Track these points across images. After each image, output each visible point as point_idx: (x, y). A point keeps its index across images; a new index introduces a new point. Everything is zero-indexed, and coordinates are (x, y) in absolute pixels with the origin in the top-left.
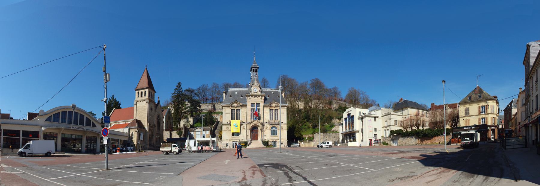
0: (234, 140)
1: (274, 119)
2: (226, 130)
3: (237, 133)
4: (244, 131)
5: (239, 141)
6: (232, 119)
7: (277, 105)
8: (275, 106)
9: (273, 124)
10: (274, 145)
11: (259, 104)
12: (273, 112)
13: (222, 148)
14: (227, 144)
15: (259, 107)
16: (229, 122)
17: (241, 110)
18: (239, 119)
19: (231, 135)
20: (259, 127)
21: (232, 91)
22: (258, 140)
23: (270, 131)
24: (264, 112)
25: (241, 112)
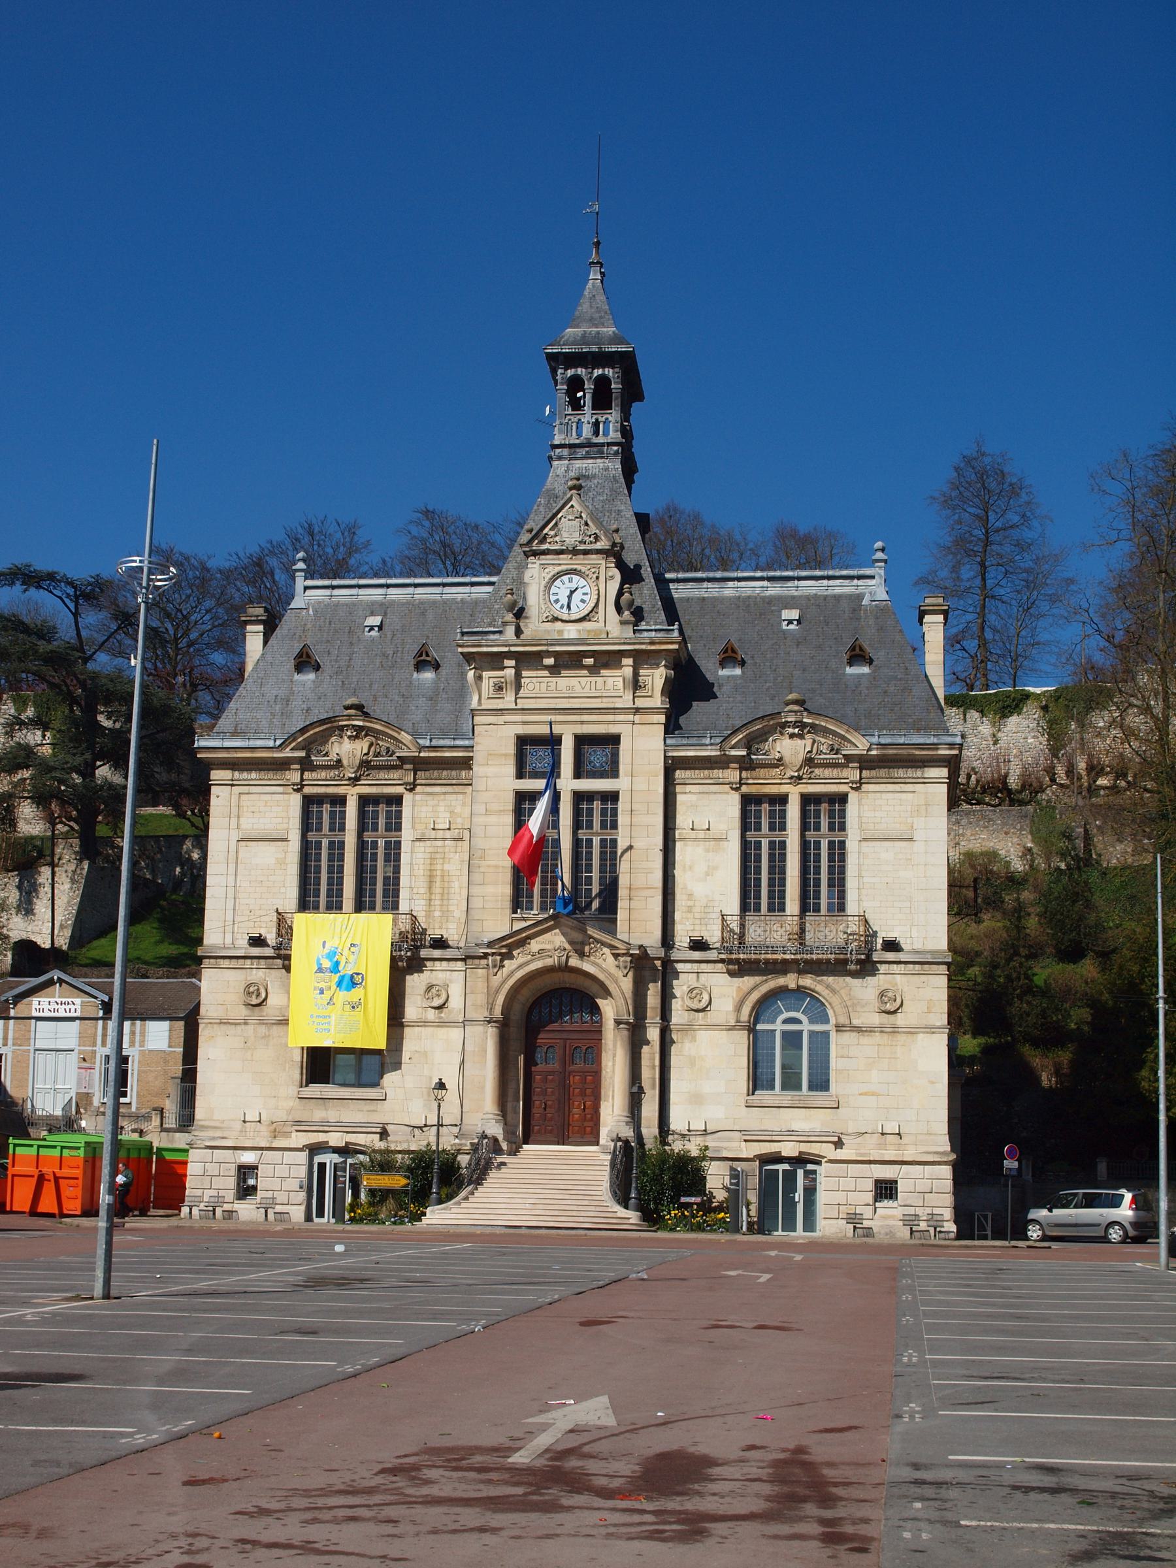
0: (325, 1126)
2: (243, 1012)
3: (361, 1053)
4: (442, 1032)
6: (306, 903)
7: (825, 743)
8: (809, 762)
9: (781, 968)
10: (790, 1205)
11: (614, 740)
14: (245, 1171)
15: (614, 773)
16: (271, 938)
18: (391, 904)
19: (296, 1074)
20: (607, 993)
23: (742, 1037)
25: (407, 835)
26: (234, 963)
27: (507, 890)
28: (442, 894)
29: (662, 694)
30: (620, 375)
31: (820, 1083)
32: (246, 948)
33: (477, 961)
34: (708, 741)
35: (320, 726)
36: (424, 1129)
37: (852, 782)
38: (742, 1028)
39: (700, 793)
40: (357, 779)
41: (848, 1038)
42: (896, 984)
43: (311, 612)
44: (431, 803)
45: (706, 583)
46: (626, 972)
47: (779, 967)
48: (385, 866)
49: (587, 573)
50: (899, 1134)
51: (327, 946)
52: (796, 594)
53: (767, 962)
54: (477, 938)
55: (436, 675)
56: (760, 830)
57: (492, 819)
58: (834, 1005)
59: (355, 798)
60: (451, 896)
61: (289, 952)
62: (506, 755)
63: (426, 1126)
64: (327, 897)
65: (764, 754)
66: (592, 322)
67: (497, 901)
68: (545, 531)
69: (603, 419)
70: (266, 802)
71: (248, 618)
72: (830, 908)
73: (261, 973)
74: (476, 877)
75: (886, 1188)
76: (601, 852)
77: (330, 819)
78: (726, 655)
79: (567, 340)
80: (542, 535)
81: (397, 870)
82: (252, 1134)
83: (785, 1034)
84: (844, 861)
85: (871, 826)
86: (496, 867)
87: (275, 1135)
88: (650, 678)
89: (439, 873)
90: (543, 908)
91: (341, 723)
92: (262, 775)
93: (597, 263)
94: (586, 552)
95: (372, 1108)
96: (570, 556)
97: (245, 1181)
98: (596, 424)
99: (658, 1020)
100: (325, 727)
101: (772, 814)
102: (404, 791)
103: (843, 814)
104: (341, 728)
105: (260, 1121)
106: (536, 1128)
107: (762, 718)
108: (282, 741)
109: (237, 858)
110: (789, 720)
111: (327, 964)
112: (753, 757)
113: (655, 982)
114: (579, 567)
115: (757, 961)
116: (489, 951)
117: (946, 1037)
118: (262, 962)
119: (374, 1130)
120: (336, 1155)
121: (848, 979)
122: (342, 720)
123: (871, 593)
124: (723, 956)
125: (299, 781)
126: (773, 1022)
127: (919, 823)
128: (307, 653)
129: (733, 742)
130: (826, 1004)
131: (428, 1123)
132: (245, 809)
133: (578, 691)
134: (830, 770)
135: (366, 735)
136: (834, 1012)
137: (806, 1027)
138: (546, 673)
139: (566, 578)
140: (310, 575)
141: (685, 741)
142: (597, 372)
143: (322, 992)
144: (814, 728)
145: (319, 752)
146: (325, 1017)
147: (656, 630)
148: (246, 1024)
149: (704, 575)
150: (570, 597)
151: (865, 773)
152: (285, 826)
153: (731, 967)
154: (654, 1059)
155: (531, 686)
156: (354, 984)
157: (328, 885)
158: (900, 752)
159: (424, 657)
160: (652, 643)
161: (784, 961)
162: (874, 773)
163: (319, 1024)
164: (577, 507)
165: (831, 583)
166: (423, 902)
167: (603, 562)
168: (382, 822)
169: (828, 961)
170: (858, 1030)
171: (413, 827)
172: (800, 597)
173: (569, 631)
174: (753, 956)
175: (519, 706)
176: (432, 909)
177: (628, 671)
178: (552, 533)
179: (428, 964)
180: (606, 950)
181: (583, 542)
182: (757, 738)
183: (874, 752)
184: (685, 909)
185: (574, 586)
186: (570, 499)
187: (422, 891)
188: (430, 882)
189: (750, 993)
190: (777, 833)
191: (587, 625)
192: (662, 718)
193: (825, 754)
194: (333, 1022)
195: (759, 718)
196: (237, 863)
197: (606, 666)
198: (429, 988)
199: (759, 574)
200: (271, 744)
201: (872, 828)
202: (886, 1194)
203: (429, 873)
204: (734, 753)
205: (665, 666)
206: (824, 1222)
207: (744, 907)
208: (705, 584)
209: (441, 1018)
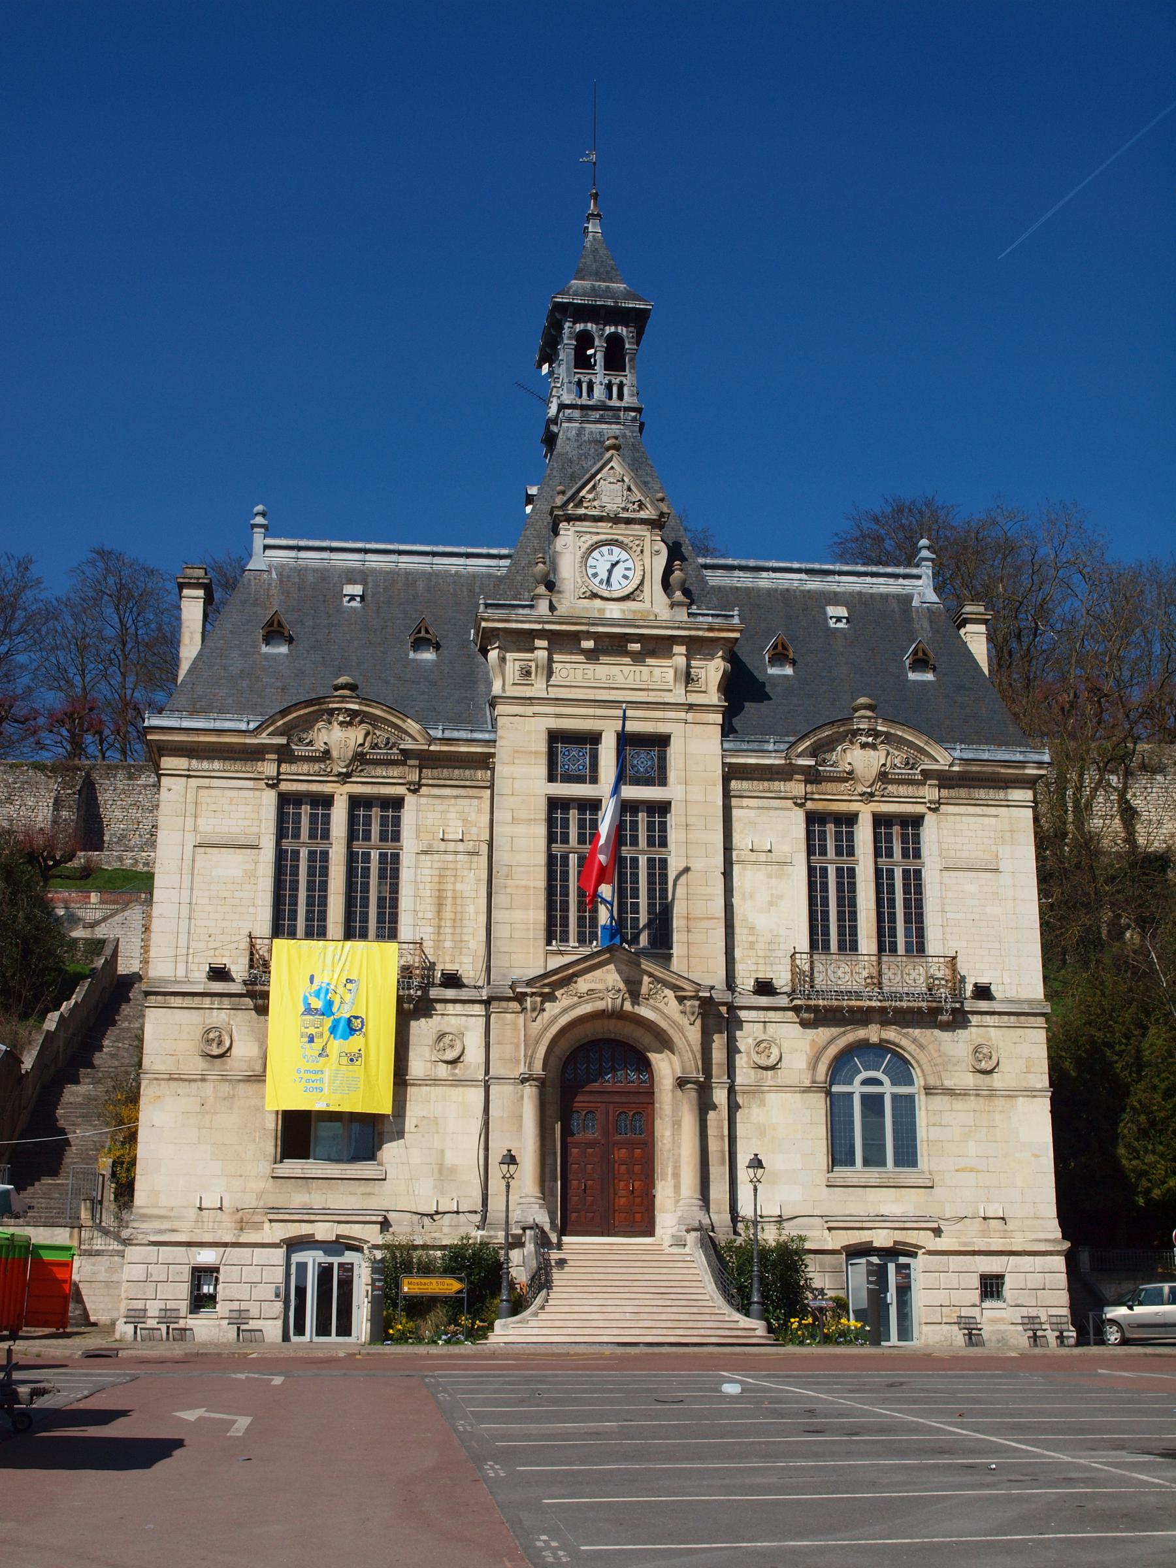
0: (309, 1215)
1: (867, 941)
2: (199, 1065)
4: (457, 1093)
5: (371, 1234)
6: (281, 927)
7: (899, 758)
8: (883, 777)
9: (862, 1017)
11: (663, 741)
12: (847, 848)
13: (124, 1330)
15: (663, 782)
16: (239, 969)
17: (408, 816)
18: (389, 931)
19: (269, 1146)
21: (301, 572)
22: (650, 1232)
23: (819, 1102)
24: (728, 848)
26: (188, 1002)
27: (541, 916)
28: (454, 920)
29: (718, 690)
30: (635, 335)
31: (907, 1155)
32: (205, 983)
33: (504, 1004)
34: (771, 747)
35: (306, 707)
36: (436, 1217)
37: (931, 802)
38: (819, 1089)
39: (759, 808)
40: (348, 775)
41: (939, 1102)
42: (990, 1039)
43: (274, 575)
44: (438, 808)
45: (737, 571)
46: (692, 1019)
47: (858, 1016)
48: (380, 884)
49: (631, 545)
50: (1003, 1219)
51: (316, 980)
52: (838, 590)
53: (851, 1010)
54: (504, 975)
55: (437, 656)
56: (825, 854)
57: (521, 829)
58: (922, 1062)
59: (345, 798)
60: (466, 923)
61: (266, 988)
62: (536, 753)
63: (437, 1213)
64: (307, 920)
65: (832, 766)
66: (598, 276)
67: (528, 929)
68: (581, 494)
69: (617, 381)
70: (231, 799)
71: (187, 580)
72: (908, 949)
73: (223, 1015)
74: (498, 899)
75: (991, 1284)
76: (649, 874)
77: (311, 823)
78: (776, 651)
79: (576, 291)
80: (578, 499)
81: (395, 888)
82: (211, 1225)
83: (865, 1098)
84: (921, 894)
85: (952, 854)
86: (526, 887)
87: (242, 1225)
88: (703, 670)
89: (449, 894)
90: (581, 940)
91: (331, 706)
92: (228, 765)
93: (599, 215)
94: (629, 521)
95: (368, 1190)
96: (610, 525)
97: (199, 1287)
98: (609, 386)
99: (725, 1078)
100: (311, 709)
101: (838, 836)
102: (406, 792)
103: (917, 838)
104: (331, 712)
105: (221, 1209)
106: (574, 1215)
107: (833, 723)
108: (257, 724)
109: (193, 868)
110: (862, 727)
111: (317, 1004)
112: (820, 768)
113: (721, 1032)
114: (620, 538)
115: (840, 1009)
116: (528, 990)
117: (1047, 1102)
118: (226, 1000)
119: (374, 1219)
120: (320, 1253)
121: (937, 1032)
122: (334, 702)
123: (919, 594)
124: (797, 1002)
125: (275, 774)
126: (850, 1083)
127: (1004, 851)
128: (279, 621)
129: (799, 750)
130: (913, 1061)
131: (440, 1210)
132: (204, 807)
133: (620, 681)
134: (905, 787)
135: (361, 722)
136: (923, 1071)
137: (888, 1089)
138: (581, 658)
139: (605, 549)
140: (268, 531)
141: (745, 746)
142: (609, 330)
143: (311, 1039)
144: (889, 738)
145: (301, 740)
146: (316, 1072)
147: (713, 615)
148: (203, 1080)
149: (736, 563)
150: (610, 572)
151: (944, 792)
152: (255, 830)
153: (806, 1016)
154: (722, 1128)
155: (564, 673)
156: (352, 1031)
157: (307, 905)
158: (984, 769)
159: (423, 634)
160: (710, 629)
161: (870, 1009)
162: (953, 793)
163: (308, 1081)
164: (619, 469)
165: (875, 580)
166: (431, 930)
167: (648, 534)
168: (375, 829)
169: (920, 1008)
170: (951, 1092)
171: (418, 837)
172: (844, 593)
173: (611, 609)
174: (836, 1003)
175: (551, 696)
176: (442, 938)
177: (681, 661)
178: (590, 496)
179: (438, 1006)
180: (669, 993)
181: (625, 509)
182: (823, 746)
183: (956, 768)
184: (746, 945)
185: (614, 559)
186: (610, 460)
187: (429, 915)
188: (440, 905)
189: (825, 1048)
190: (845, 858)
191: (629, 604)
192: (719, 718)
193: (900, 768)
194: (326, 1080)
195: (828, 724)
196: (192, 874)
197: (653, 654)
198: (441, 1036)
199: (796, 565)
200: (243, 726)
201: (954, 856)
202: (992, 1292)
203: (437, 894)
204: (801, 762)
205: (723, 658)
206: (925, 1328)
207: (813, 945)
208: (737, 573)
209: (456, 1075)
